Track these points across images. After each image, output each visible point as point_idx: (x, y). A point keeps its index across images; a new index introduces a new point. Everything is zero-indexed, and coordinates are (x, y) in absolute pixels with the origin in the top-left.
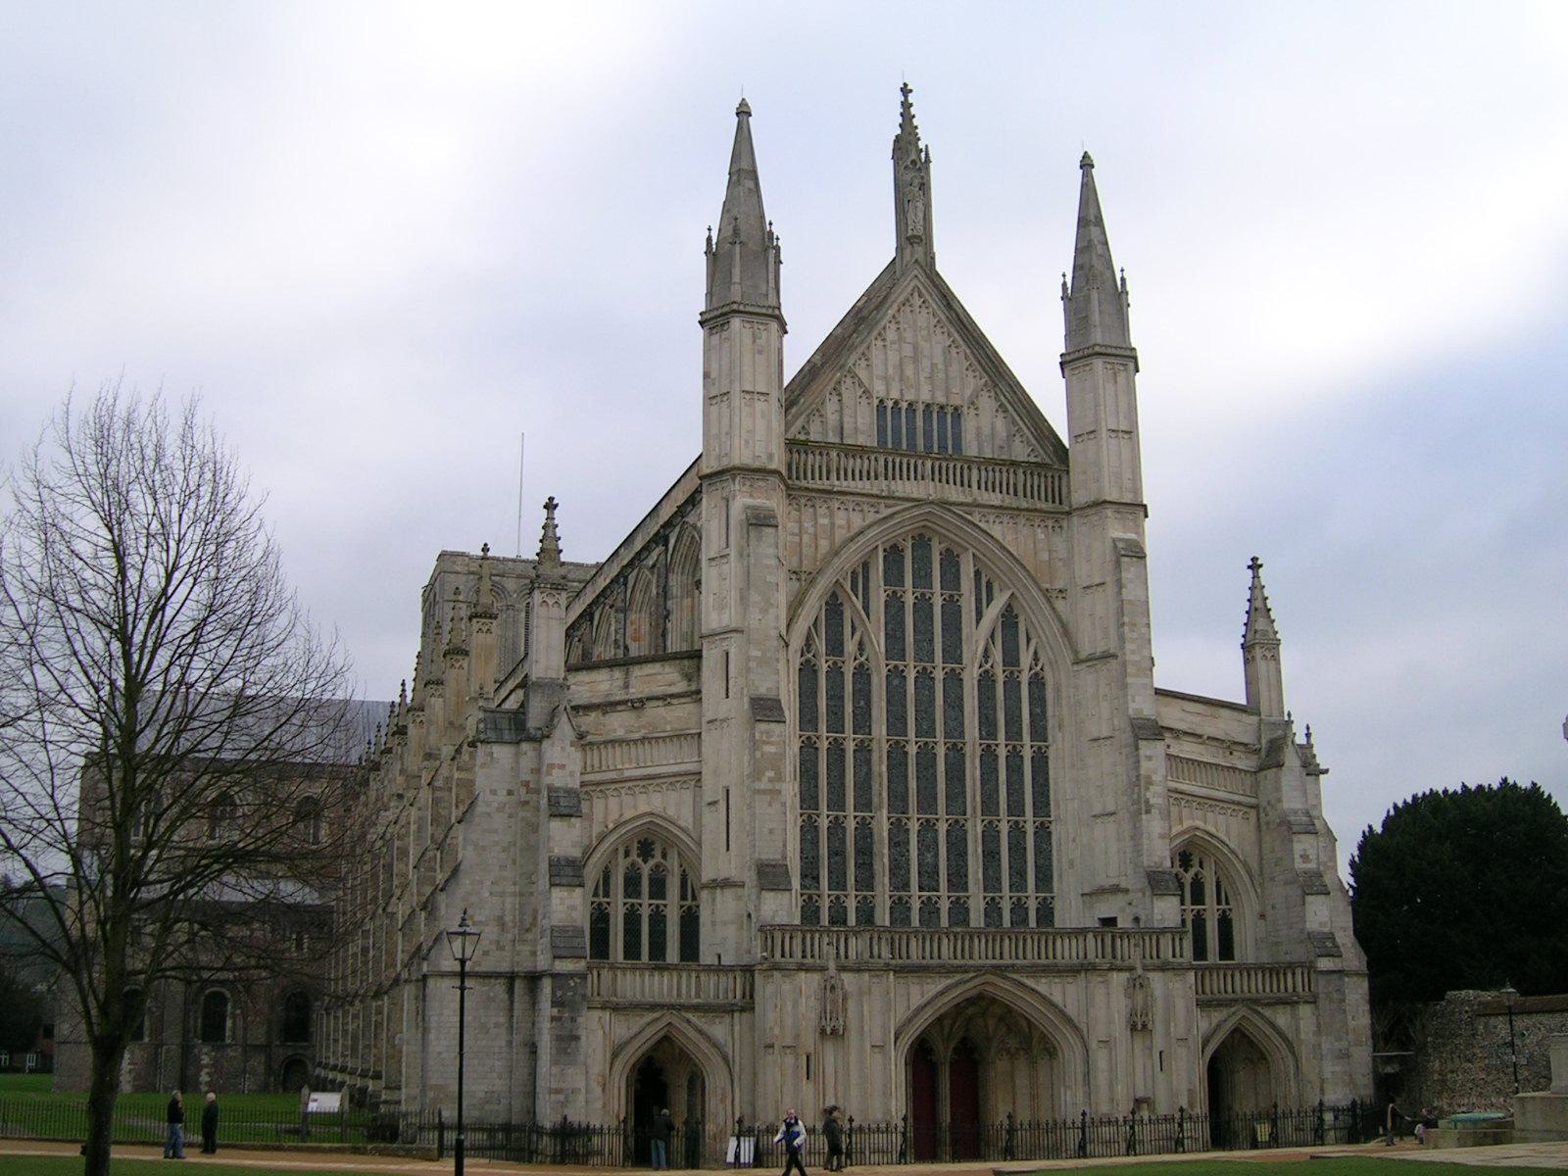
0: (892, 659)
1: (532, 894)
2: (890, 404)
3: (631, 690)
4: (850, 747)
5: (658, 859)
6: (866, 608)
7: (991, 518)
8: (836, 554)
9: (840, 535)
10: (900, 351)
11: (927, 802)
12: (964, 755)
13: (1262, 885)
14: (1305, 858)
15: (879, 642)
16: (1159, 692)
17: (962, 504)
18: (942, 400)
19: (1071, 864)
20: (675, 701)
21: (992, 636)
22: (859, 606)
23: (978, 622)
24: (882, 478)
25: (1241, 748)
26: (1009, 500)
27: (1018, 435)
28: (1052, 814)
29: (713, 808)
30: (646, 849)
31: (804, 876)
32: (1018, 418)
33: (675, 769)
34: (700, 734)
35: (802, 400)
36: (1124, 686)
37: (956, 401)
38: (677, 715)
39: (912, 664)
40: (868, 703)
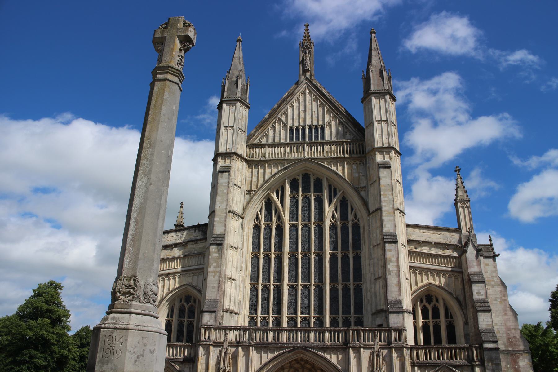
0: (292, 221)
2: (294, 128)
5: (192, 302)
6: (282, 203)
12: (323, 258)
13: (466, 308)
14: (479, 293)
16: (408, 226)
18: (315, 123)
19: (368, 300)
20: (199, 242)
22: (278, 202)
27: (348, 132)
28: (363, 281)
30: (188, 298)
31: (251, 309)
32: (347, 126)
33: (196, 267)
35: (259, 131)
36: (381, 221)
37: (320, 123)
38: (200, 245)
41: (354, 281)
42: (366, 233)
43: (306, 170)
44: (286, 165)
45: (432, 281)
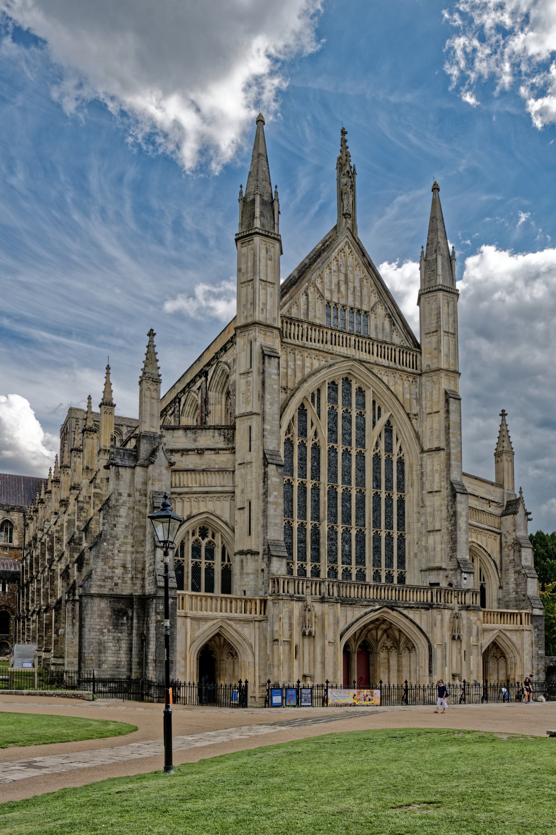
1: (142, 552)
3: (197, 444)
4: (309, 486)
7: (383, 372)
8: (304, 381)
9: (307, 371)
10: (338, 277)
11: (347, 519)
13: (501, 573)
15: (324, 434)
17: (369, 363)
18: (358, 305)
20: (221, 452)
21: (380, 436)
22: (315, 410)
23: (374, 426)
24: (329, 343)
25: (495, 504)
26: (392, 364)
28: (406, 530)
29: (241, 511)
33: (220, 489)
34: (234, 472)
37: (365, 308)
38: (223, 459)
39: (341, 446)
40: (319, 464)
41: (398, 530)
42: (414, 473)
43: (349, 373)
44: (331, 362)
45: (474, 540)
